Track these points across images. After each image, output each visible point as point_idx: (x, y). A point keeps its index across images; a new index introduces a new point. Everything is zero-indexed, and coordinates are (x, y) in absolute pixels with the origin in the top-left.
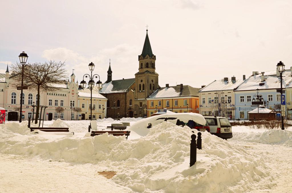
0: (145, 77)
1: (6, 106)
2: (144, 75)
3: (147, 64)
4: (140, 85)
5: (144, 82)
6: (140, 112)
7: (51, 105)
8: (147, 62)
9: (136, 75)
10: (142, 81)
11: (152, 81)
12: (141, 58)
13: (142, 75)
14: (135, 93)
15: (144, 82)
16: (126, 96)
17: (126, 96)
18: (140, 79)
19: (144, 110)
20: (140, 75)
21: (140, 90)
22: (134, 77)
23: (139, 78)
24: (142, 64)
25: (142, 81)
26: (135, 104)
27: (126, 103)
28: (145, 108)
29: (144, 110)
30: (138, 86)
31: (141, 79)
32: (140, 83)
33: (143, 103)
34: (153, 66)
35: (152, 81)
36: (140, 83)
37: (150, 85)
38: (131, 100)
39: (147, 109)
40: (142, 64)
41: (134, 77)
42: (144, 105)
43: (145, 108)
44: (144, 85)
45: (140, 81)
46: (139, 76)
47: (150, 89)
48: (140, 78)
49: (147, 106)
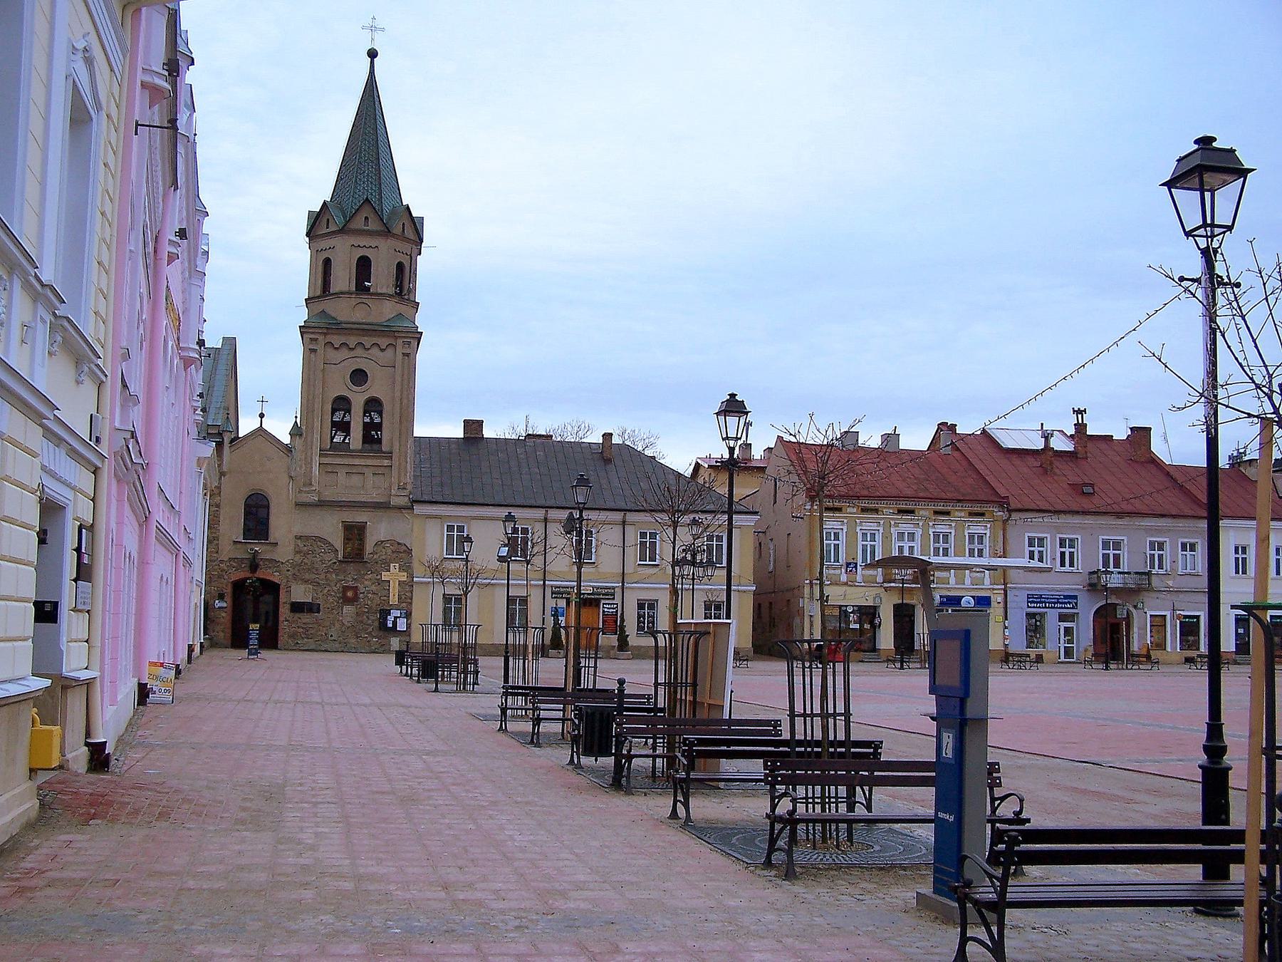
2: (384, 342)
3: (364, 266)
4: (342, 403)
6: (346, 589)
10: (359, 377)
13: (368, 341)
14: (298, 455)
15: (376, 388)
19: (385, 576)
20: (352, 341)
25: (359, 377)
26: (298, 529)
28: (395, 568)
29: (385, 576)
33: (380, 530)
34: (404, 277)
39: (407, 567)
42: (380, 543)
43: (395, 568)
44: (373, 405)
46: (337, 340)
48: (344, 353)
49: (409, 551)
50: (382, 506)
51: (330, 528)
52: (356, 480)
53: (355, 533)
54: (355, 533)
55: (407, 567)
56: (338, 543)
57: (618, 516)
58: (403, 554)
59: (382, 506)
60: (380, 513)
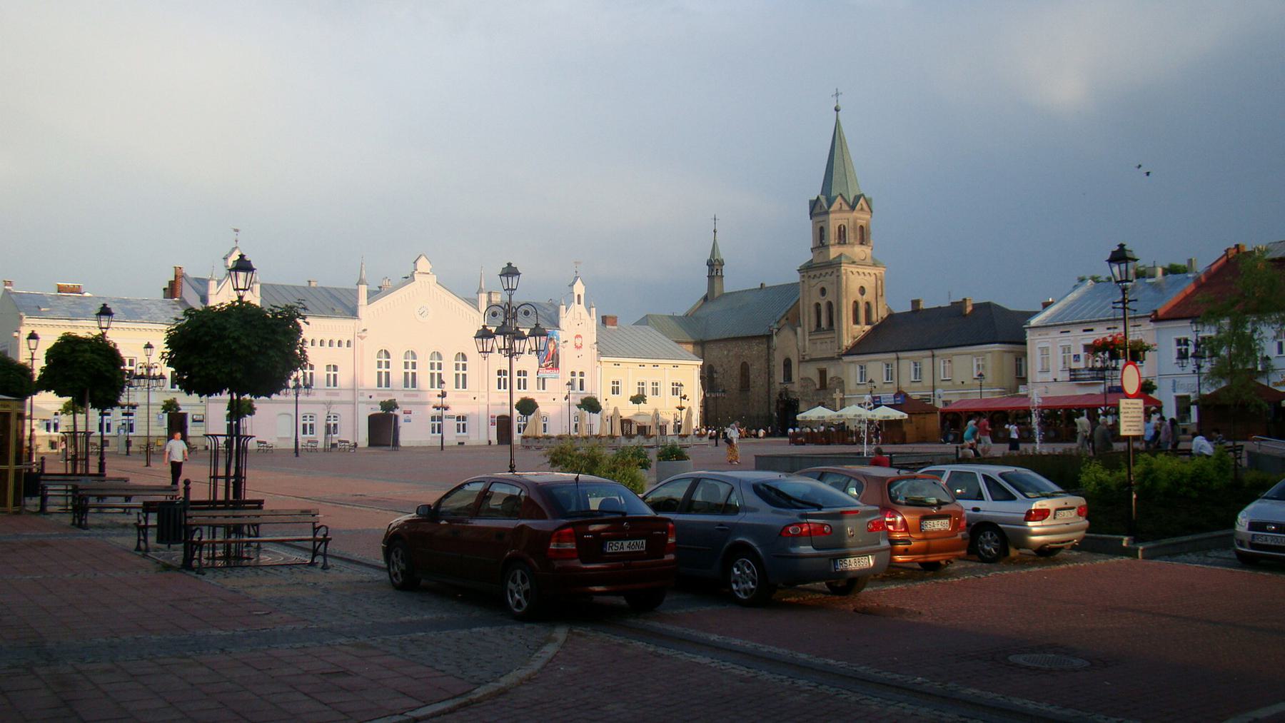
0: (834, 276)
1: (362, 395)
2: (829, 271)
4: (818, 305)
5: (830, 297)
7: (464, 387)
8: (841, 222)
9: (807, 269)
10: (823, 291)
11: (862, 291)
12: (817, 210)
13: (823, 272)
15: (830, 297)
16: (769, 348)
17: (769, 348)
18: (816, 284)
20: (818, 273)
21: (819, 324)
22: (796, 278)
23: (813, 282)
24: (822, 229)
25: (823, 291)
27: (770, 374)
30: (813, 310)
31: (819, 286)
32: (816, 297)
33: (831, 373)
35: (862, 291)
36: (816, 297)
37: (856, 303)
38: (787, 364)
39: (843, 391)
40: (822, 229)
41: (796, 278)
45: (816, 292)
46: (812, 274)
47: (856, 321)
48: (816, 280)
50: (832, 359)
51: (812, 372)
52: (824, 346)
53: (823, 373)
54: (823, 373)
55: (843, 391)
56: (816, 380)
57: (928, 353)
58: (841, 383)
59: (832, 359)
60: (831, 363)
